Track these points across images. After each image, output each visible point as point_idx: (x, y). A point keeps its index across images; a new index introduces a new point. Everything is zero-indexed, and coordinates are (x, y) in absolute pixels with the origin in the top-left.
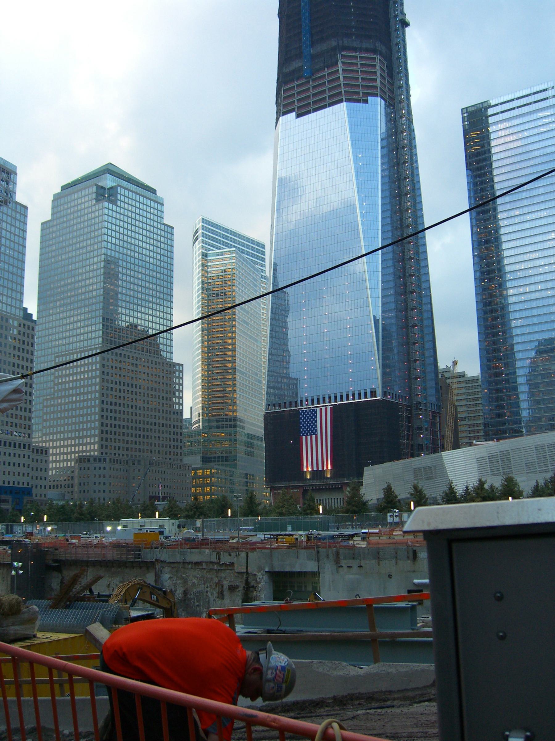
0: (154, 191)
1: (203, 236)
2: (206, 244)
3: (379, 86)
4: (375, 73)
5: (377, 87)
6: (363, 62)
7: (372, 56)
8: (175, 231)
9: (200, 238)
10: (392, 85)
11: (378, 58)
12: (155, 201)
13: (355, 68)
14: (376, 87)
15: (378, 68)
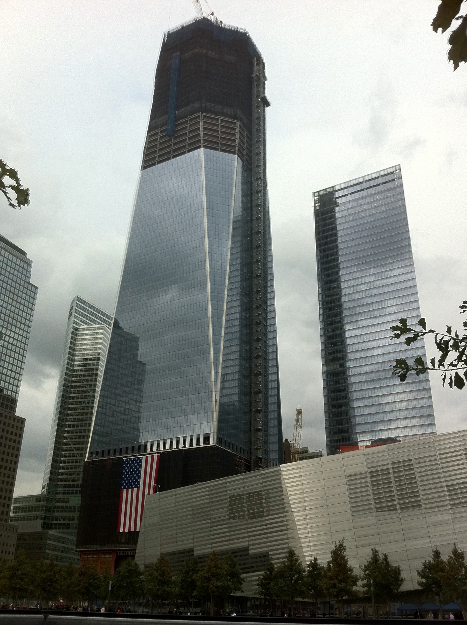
0: (24, 253)
1: (76, 312)
2: (78, 320)
3: (237, 146)
4: (235, 135)
5: (235, 147)
6: (224, 124)
7: (233, 120)
8: (39, 292)
9: (74, 314)
10: (250, 152)
11: (238, 123)
12: (21, 260)
13: (215, 128)
14: (235, 147)
15: (238, 131)
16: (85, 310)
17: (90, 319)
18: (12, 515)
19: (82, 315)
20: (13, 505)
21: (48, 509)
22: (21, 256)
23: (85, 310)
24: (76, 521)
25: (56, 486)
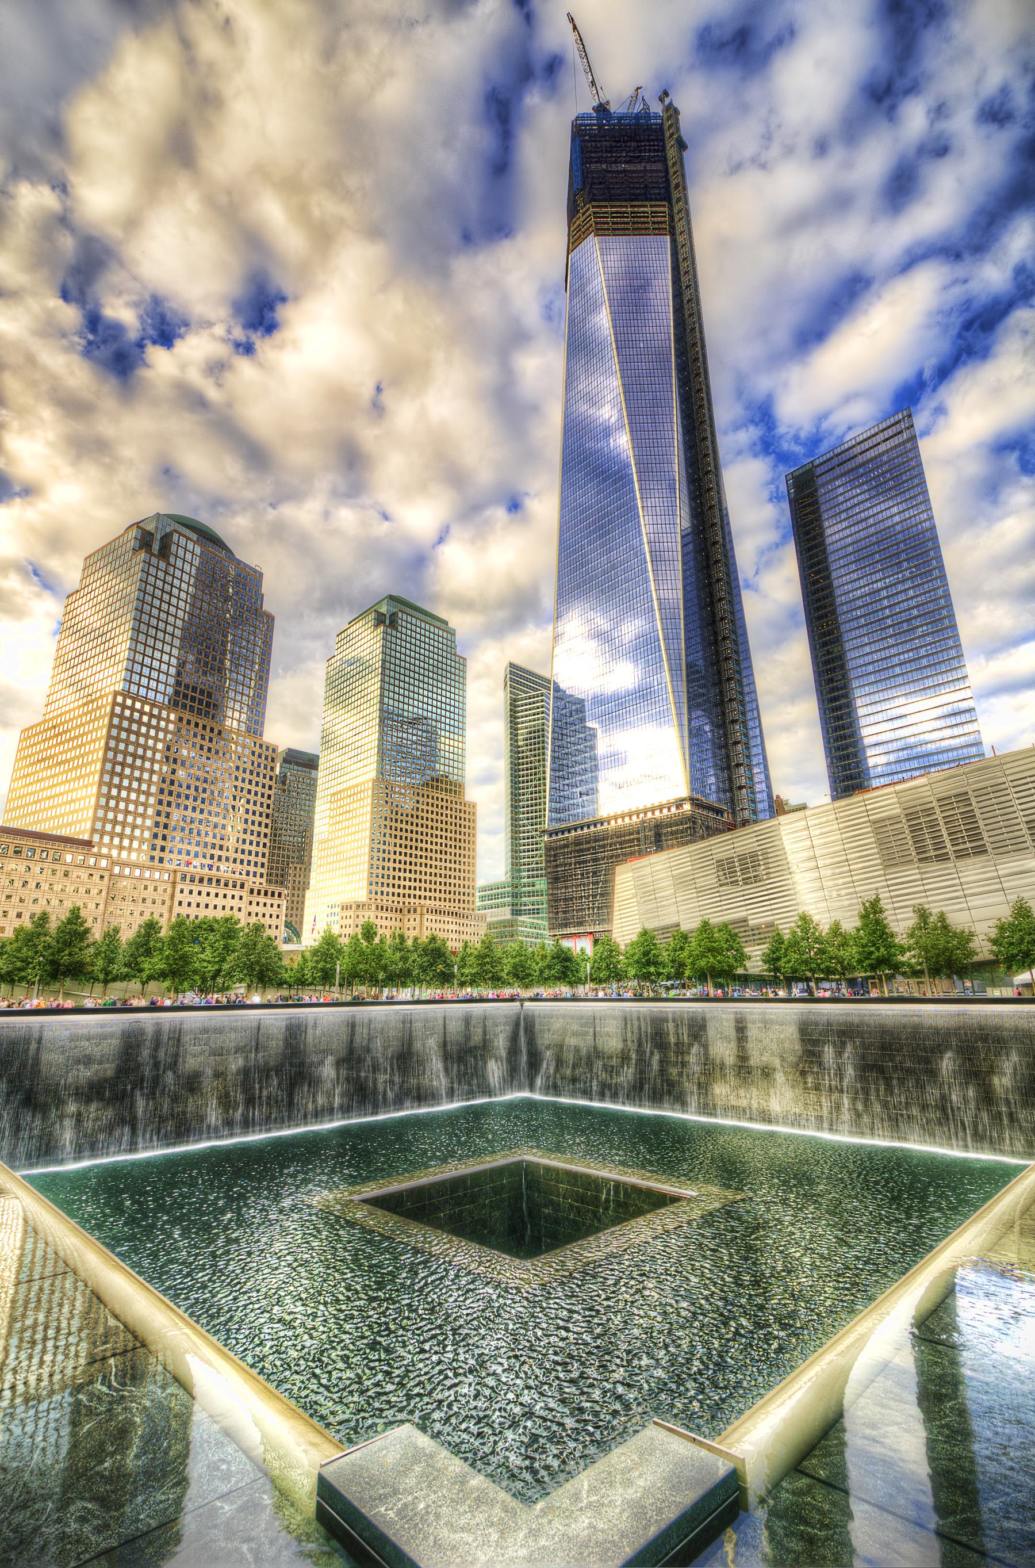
16: (521, 677)
17: (527, 686)
18: (478, 904)
19: (518, 682)
20: (477, 894)
21: (515, 896)
22: (443, 626)
23: (521, 677)
24: (545, 906)
25: (519, 871)
